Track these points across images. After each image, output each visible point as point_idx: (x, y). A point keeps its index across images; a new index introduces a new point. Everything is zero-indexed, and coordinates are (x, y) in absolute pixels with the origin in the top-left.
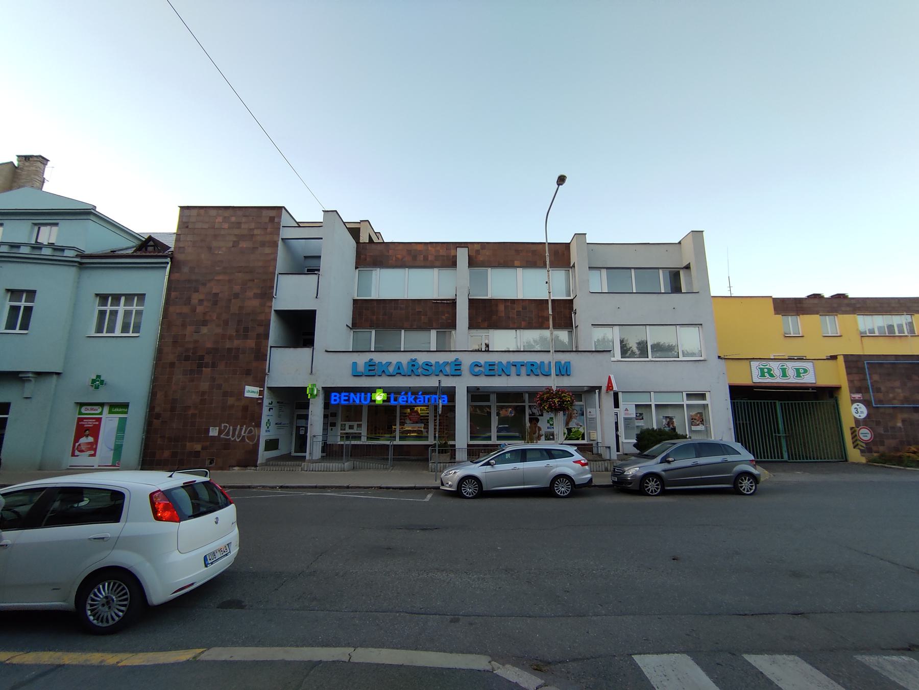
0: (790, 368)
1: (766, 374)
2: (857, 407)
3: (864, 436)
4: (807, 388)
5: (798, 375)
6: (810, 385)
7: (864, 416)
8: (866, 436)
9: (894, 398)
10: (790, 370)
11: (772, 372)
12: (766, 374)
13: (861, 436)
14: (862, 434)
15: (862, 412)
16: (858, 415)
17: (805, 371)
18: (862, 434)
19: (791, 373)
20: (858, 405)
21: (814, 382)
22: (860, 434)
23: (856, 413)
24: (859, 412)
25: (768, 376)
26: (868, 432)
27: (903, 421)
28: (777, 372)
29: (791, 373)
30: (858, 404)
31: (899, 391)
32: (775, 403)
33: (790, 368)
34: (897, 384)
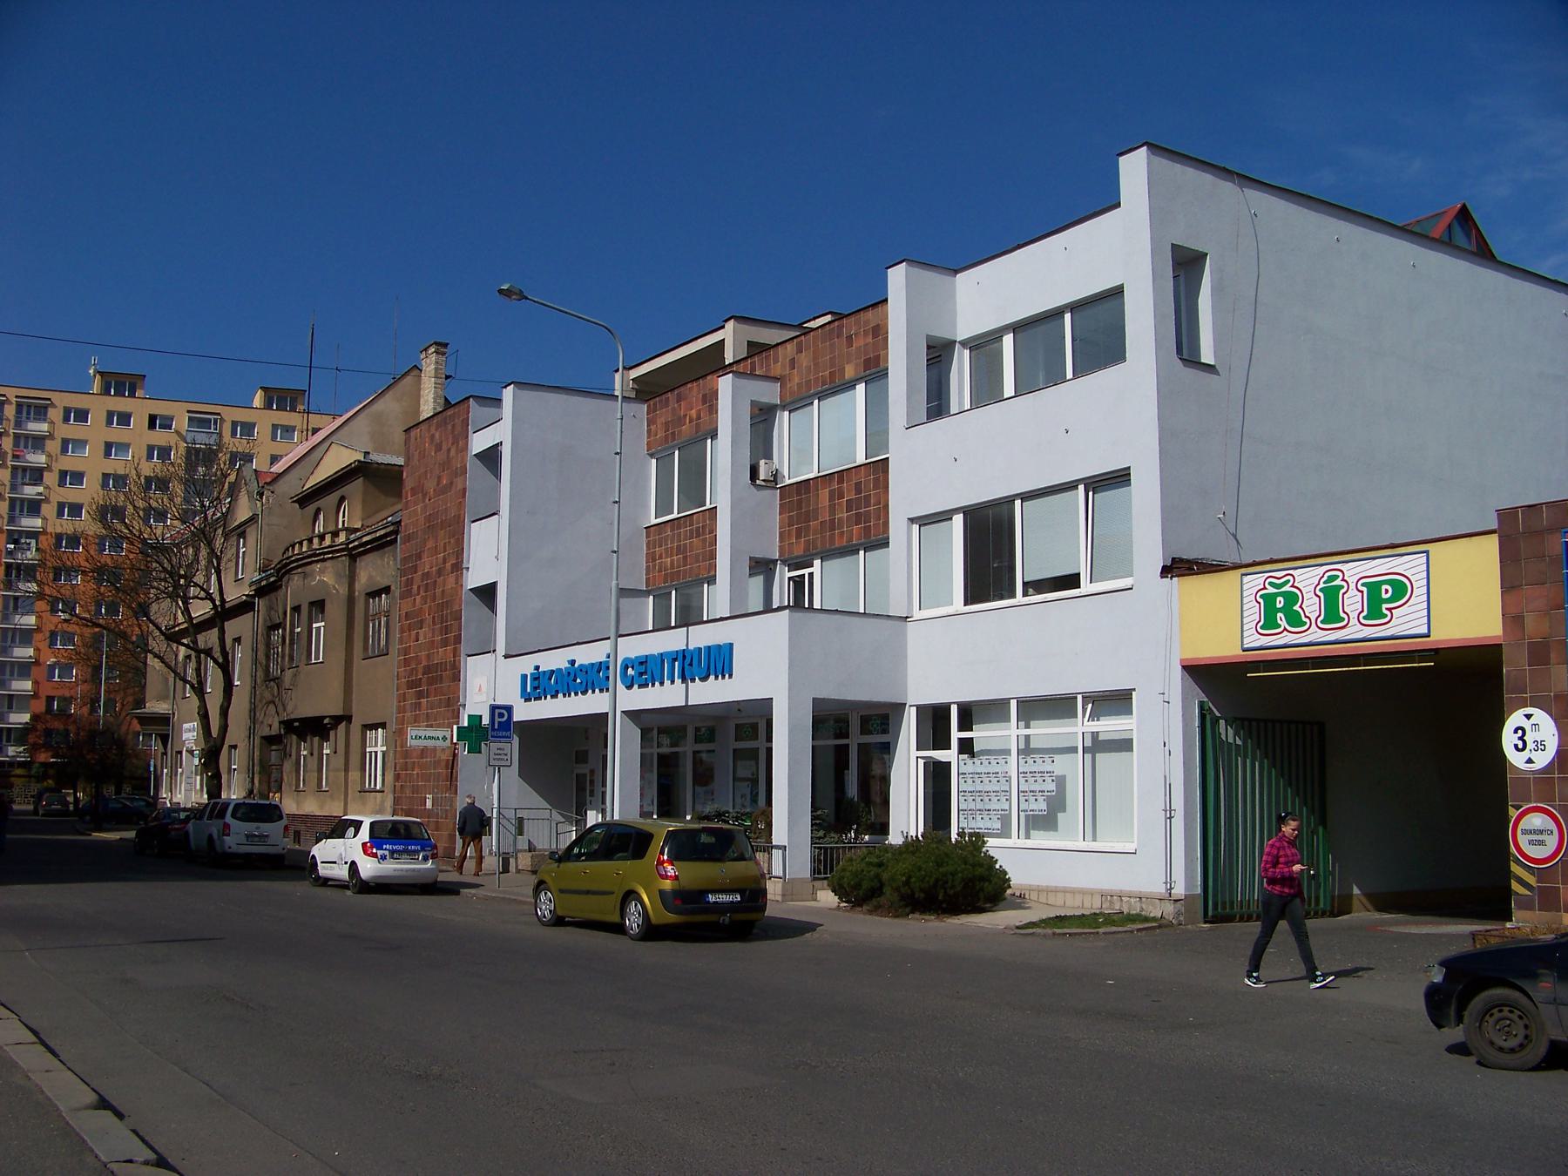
0: (1352, 586)
1: (1279, 615)
2: (1526, 724)
3: (1530, 842)
5: (1374, 609)
7: (1542, 759)
8: (1541, 843)
10: (1353, 591)
11: (1296, 608)
12: (1279, 615)
13: (1523, 840)
14: (1525, 832)
15: (1540, 746)
16: (1525, 755)
17: (1400, 590)
18: (1525, 832)
19: (1353, 603)
20: (1528, 717)
21: (1424, 630)
23: (1516, 746)
24: (1530, 745)
25: (1284, 624)
26: (1552, 825)
28: (1311, 606)
29: (1353, 603)
30: (1529, 710)
33: (1352, 586)
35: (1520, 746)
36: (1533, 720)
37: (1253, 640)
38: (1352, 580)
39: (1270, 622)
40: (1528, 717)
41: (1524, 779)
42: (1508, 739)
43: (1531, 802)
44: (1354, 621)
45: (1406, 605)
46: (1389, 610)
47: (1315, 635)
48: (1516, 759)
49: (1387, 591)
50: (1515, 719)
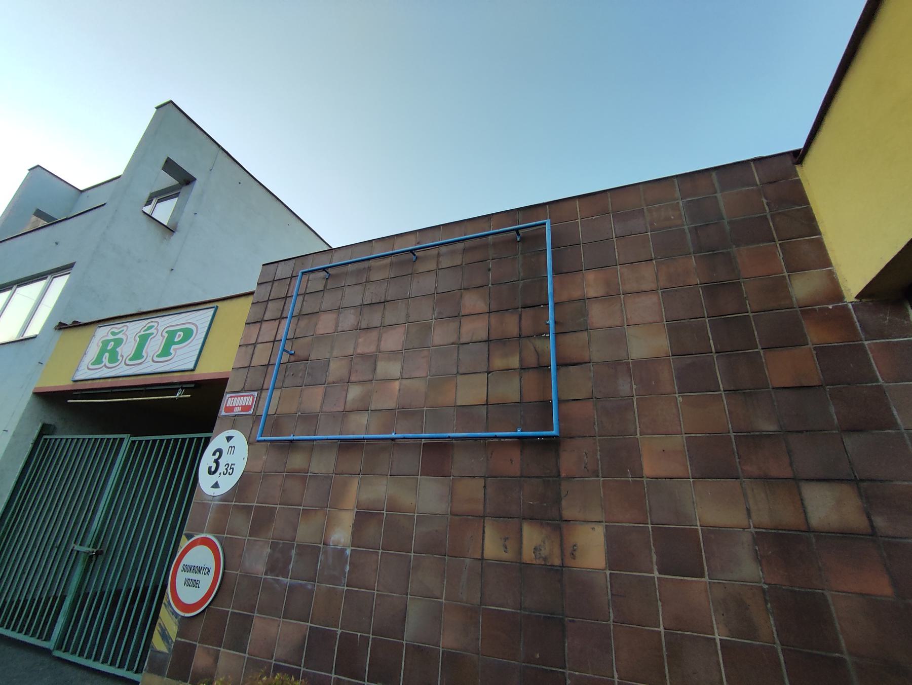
2: (225, 446)
4: (170, 388)
5: (166, 352)
6: (176, 378)
7: (227, 483)
9: (363, 408)
13: (181, 576)
19: (154, 346)
22: (181, 568)
23: (210, 468)
24: (222, 468)
26: (212, 564)
27: (364, 516)
28: (127, 349)
31: (392, 368)
32: (122, 440)
34: (393, 340)
35: (213, 469)
36: (232, 443)
37: (84, 373)
38: (161, 329)
39: (98, 360)
40: (229, 438)
41: (205, 506)
42: (207, 460)
43: (202, 532)
44: (150, 359)
45: (189, 345)
46: (175, 350)
47: (122, 369)
48: (205, 481)
49: (180, 335)
50: (218, 441)
